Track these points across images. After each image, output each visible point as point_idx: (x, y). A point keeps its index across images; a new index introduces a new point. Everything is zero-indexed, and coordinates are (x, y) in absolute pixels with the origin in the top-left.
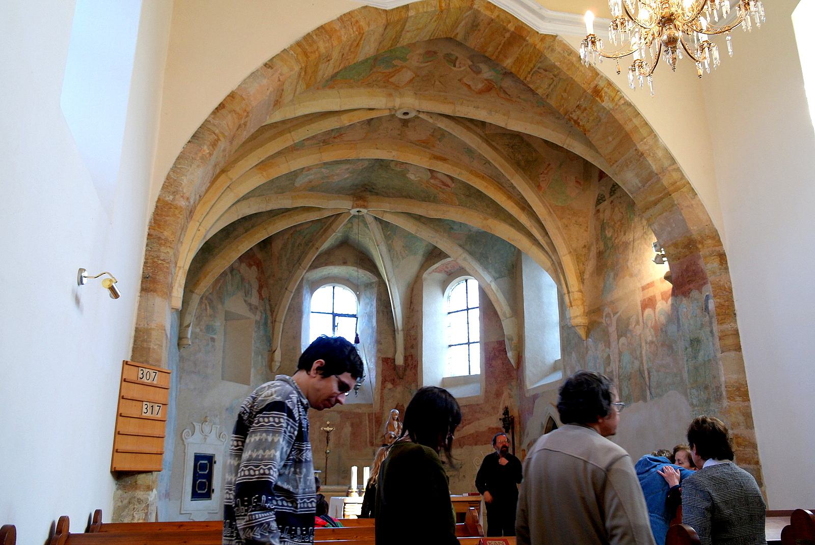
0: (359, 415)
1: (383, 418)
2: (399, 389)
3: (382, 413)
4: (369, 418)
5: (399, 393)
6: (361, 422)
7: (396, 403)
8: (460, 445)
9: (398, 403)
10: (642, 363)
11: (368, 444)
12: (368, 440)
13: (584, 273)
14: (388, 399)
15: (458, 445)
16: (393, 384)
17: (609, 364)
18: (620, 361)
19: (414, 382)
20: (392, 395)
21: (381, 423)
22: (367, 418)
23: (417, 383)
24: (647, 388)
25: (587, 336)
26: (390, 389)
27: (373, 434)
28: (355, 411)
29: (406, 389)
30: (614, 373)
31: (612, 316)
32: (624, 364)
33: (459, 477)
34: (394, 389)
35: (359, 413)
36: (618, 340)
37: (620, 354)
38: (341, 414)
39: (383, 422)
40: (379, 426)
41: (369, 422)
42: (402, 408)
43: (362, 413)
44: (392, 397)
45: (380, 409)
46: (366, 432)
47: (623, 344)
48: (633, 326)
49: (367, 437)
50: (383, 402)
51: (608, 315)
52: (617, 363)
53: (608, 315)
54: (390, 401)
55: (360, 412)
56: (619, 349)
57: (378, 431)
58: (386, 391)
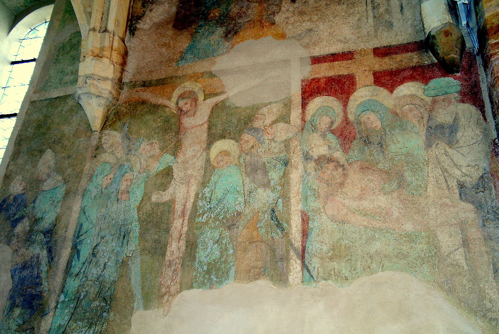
10: (285, 197)
13: (139, 18)
17: (164, 187)
18: (204, 184)
24: (292, 253)
25: (108, 122)
30: (178, 207)
31: (201, 97)
32: (219, 193)
36: (210, 144)
37: (209, 168)
47: (226, 153)
48: (268, 122)
51: (192, 96)
52: (194, 189)
53: (192, 96)
56: (208, 160)
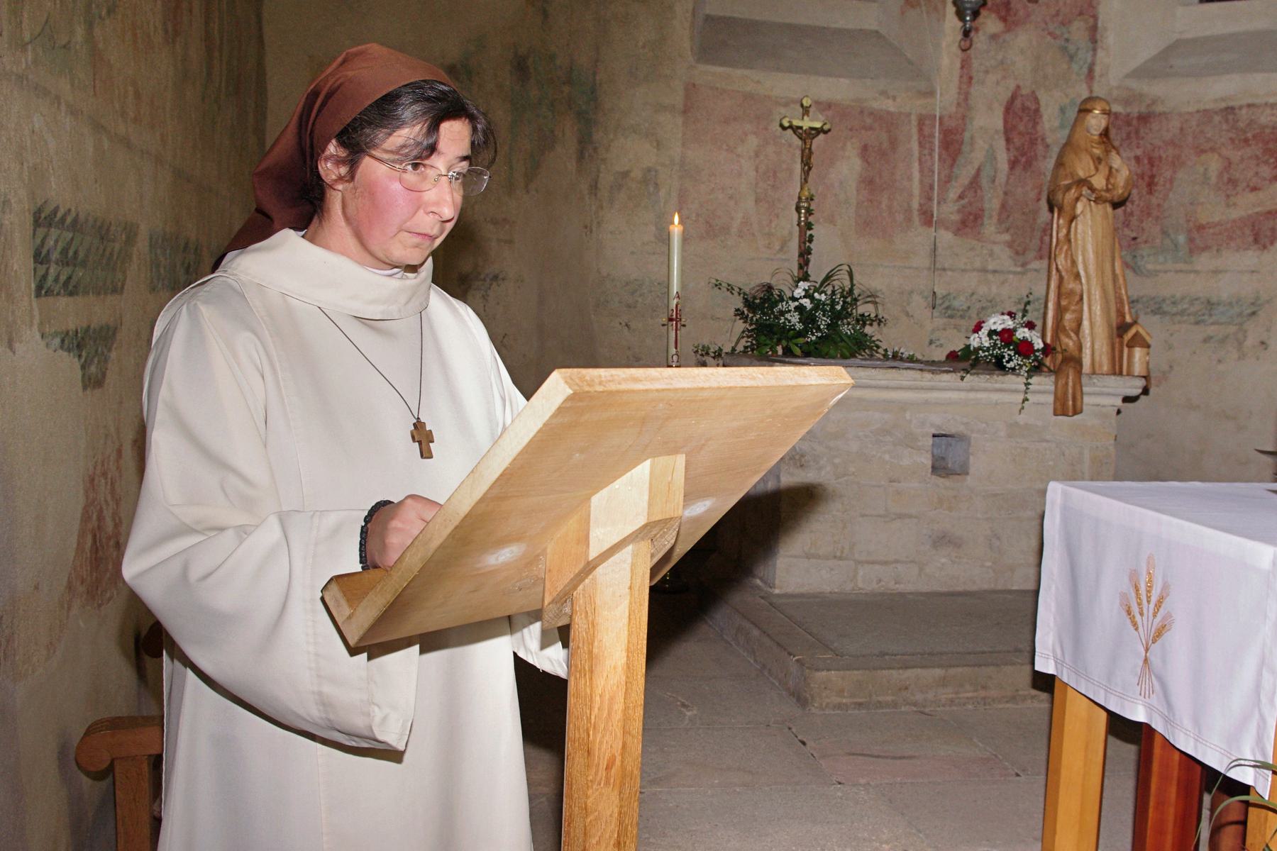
0: (888, 122)
1: (967, 135)
2: (1023, 38)
3: (964, 117)
4: (920, 130)
5: (1022, 52)
6: (893, 143)
7: (1012, 86)
8: (1256, 241)
9: (1018, 87)
11: (916, 213)
12: (915, 205)
14: (987, 72)
15: (1251, 239)
16: (1004, 20)
19: (1081, 14)
20: (1000, 57)
21: (959, 152)
22: (914, 131)
23: (1095, 17)
26: (994, 37)
27: (932, 187)
28: (876, 105)
29: (1049, 38)
33: (1240, 344)
34: (1008, 37)
35: (888, 113)
38: (830, 113)
39: (965, 148)
40: (954, 160)
41: (921, 145)
42: (1028, 104)
43: (900, 113)
44: (1002, 63)
45: (959, 104)
46: (910, 179)
49: (911, 195)
50: (971, 78)
54: (992, 78)
55: (892, 109)
57: (947, 181)
58: (980, 40)
